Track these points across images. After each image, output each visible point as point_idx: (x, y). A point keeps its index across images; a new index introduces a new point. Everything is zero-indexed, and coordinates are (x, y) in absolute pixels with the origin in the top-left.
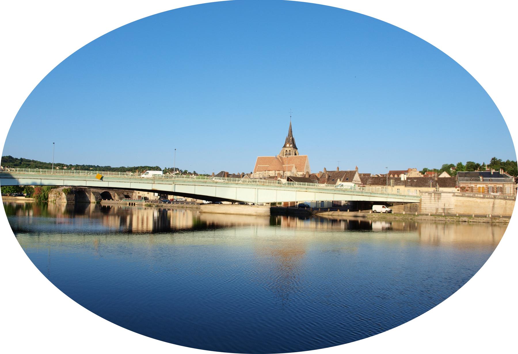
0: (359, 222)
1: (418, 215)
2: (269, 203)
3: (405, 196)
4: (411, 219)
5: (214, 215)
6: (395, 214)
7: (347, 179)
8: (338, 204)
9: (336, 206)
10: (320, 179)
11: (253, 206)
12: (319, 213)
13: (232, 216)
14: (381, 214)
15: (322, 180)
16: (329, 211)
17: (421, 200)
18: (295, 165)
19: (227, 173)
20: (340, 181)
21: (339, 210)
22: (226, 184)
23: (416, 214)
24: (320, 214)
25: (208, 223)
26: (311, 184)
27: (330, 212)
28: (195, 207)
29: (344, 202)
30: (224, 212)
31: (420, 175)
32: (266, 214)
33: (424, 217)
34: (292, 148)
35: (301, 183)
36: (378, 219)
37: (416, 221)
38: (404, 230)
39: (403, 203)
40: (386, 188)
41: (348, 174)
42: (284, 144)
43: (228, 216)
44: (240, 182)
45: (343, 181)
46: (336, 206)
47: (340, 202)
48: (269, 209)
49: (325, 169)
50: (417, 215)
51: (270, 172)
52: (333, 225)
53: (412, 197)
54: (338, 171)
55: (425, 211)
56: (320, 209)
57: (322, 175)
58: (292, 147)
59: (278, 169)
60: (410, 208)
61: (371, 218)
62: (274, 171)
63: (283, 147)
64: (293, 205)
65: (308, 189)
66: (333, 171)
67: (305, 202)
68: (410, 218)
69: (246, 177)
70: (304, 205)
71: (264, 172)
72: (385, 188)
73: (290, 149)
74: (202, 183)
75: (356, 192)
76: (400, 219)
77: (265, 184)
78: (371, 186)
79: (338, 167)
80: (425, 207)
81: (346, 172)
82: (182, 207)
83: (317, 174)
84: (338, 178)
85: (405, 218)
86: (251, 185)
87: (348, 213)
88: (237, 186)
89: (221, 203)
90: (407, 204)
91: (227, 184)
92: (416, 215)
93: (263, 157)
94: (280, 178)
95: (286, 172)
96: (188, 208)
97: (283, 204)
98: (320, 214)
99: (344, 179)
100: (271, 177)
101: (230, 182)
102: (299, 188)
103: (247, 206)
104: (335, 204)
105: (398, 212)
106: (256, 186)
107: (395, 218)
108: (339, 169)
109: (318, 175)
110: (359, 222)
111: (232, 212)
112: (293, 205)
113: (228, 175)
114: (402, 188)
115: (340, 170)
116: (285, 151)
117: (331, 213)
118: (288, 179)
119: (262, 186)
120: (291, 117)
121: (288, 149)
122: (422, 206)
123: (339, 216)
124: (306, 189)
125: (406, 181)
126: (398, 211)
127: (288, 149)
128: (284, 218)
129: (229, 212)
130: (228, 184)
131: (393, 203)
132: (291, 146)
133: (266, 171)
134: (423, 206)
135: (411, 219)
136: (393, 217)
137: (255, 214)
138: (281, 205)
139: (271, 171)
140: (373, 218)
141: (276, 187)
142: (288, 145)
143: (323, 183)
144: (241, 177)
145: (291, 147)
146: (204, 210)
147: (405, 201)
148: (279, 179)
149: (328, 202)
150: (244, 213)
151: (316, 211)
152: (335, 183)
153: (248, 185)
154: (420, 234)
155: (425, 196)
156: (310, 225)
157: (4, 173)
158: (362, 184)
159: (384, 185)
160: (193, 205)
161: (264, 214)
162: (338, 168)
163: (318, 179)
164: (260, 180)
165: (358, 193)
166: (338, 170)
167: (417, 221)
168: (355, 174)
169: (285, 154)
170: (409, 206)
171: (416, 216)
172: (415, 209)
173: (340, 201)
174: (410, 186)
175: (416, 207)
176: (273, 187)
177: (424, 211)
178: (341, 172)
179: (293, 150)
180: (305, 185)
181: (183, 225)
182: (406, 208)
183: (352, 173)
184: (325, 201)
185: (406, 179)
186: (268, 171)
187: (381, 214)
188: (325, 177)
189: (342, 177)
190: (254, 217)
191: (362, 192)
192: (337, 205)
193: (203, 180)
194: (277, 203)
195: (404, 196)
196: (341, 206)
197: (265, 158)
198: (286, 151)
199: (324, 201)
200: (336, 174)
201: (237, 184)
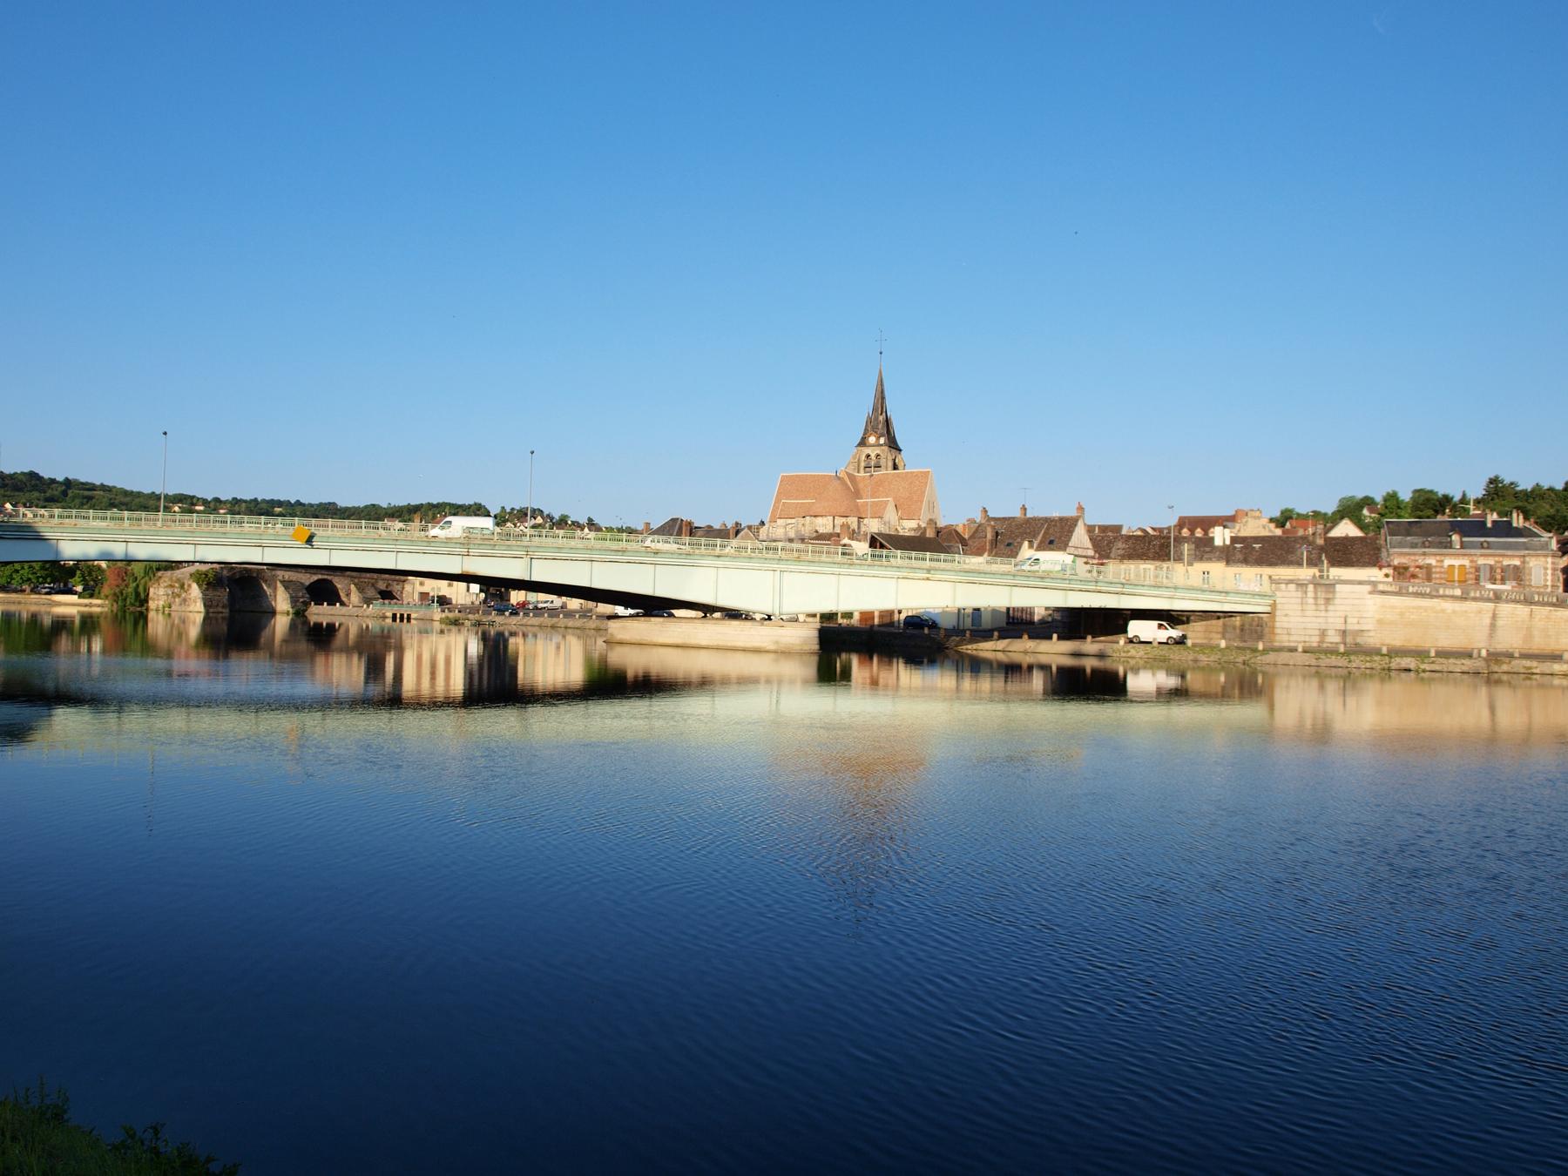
0: (1088, 670)
1: (1265, 651)
2: (814, 616)
3: (1226, 593)
4: (1244, 664)
6: (1197, 649)
7: (1051, 542)
8: (1024, 617)
9: (1018, 623)
10: (970, 542)
11: (768, 622)
12: (966, 645)
13: (703, 652)
14: (1153, 648)
15: (974, 544)
16: (998, 640)
17: (1274, 605)
18: (894, 498)
19: (690, 524)
20: (1031, 546)
21: (1026, 636)
22: (684, 556)
23: (1261, 647)
24: (970, 649)
25: (630, 674)
26: (942, 556)
27: (999, 642)
28: (593, 626)
29: (1043, 612)
30: (679, 641)
31: (1270, 531)
32: (806, 648)
33: (1284, 657)
34: (886, 448)
35: (913, 554)
36: (1146, 662)
37: (1259, 668)
38: (1223, 696)
39: (1218, 614)
40: (1168, 568)
41: (1055, 526)
42: (861, 435)
43: (693, 652)
44: (727, 550)
45: (1039, 548)
46: (1021, 623)
47: (1030, 611)
48: (816, 634)
49: (985, 511)
50: (1264, 650)
51: (819, 520)
52: (1010, 679)
53: (1248, 596)
54: (1023, 517)
55: (1285, 638)
56: (968, 632)
57: (974, 529)
59: (842, 510)
60: (1242, 630)
61: (1122, 659)
64: (888, 621)
65: (932, 572)
66: (1009, 518)
67: (923, 610)
68: (1240, 659)
69: (747, 534)
70: (922, 620)
72: (1165, 569)
73: (878, 452)
75: (1076, 580)
76: (1212, 664)
77: (803, 557)
78: (1125, 561)
79: (1024, 506)
80: (1286, 625)
81: (1046, 520)
82: (553, 627)
83: (961, 525)
84: (1023, 540)
85: (1225, 658)
87: (1055, 644)
88: (719, 563)
89: (672, 615)
90: (1233, 619)
91: (688, 557)
92: (1259, 651)
93: (797, 476)
94: (849, 538)
95: (866, 521)
96: (570, 631)
97: (856, 616)
98: (970, 649)
99: (1041, 542)
100: (820, 537)
101: (697, 551)
102: (908, 570)
103: (748, 624)
104: (1013, 618)
105: (1204, 641)
106: (777, 561)
107: (1196, 661)
108: (1028, 511)
110: (1088, 670)
111: (704, 643)
112: (887, 620)
113: (692, 530)
114: (1217, 569)
115: (1029, 515)
116: (863, 458)
117: (1002, 644)
118: (874, 542)
120: (881, 353)
121: (873, 452)
122: (1277, 624)
123: (1025, 652)
124: (929, 571)
125: (1228, 547)
126: (1205, 638)
127: (873, 452)
128: (860, 659)
129: (693, 641)
131: (1190, 616)
132: (882, 441)
134: (1281, 622)
135: (1244, 664)
136: (1190, 658)
137: (772, 647)
138: (852, 621)
139: (822, 516)
140: (1129, 660)
141: (836, 566)
142: (872, 440)
143: (979, 553)
144: (731, 536)
145: (881, 445)
146: (620, 636)
147: (1227, 608)
148: (846, 541)
149: (995, 611)
150: (740, 644)
151: (958, 639)
152: (1014, 554)
154: (1271, 707)
155: (1285, 594)
156: (939, 681)
157: (322, 574)
158: (1097, 555)
159: (1164, 560)
161: (799, 648)
162: (1024, 509)
163: (964, 542)
164: (788, 545)
165: (1083, 583)
166: (1025, 515)
167: (1263, 669)
168: (1076, 525)
169: (863, 464)
170: (1238, 623)
171: (1258, 654)
172: (1256, 632)
173: (1030, 608)
174: (1241, 562)
175: (1258, 626)
177: (1282, 639)
178: (1034, 519)
180: (924, 559)
182: (1229, 630)
183: (1066, 524)
184: (986, 608)
185: (1228, 542)
187: (1153, 648)
188: (986, 537)
189: (1035, 537)
190: (772, 656)
191: (1097, 582)
192: (1022, 620)
193: (614, 545)
194: (839, 615)
195: (1223, 594)
196: (1031, 623)
197: (802, 479)
198: (868, 456)
199: (982, 609)
200: (1019, 526)
201: (718, 556)
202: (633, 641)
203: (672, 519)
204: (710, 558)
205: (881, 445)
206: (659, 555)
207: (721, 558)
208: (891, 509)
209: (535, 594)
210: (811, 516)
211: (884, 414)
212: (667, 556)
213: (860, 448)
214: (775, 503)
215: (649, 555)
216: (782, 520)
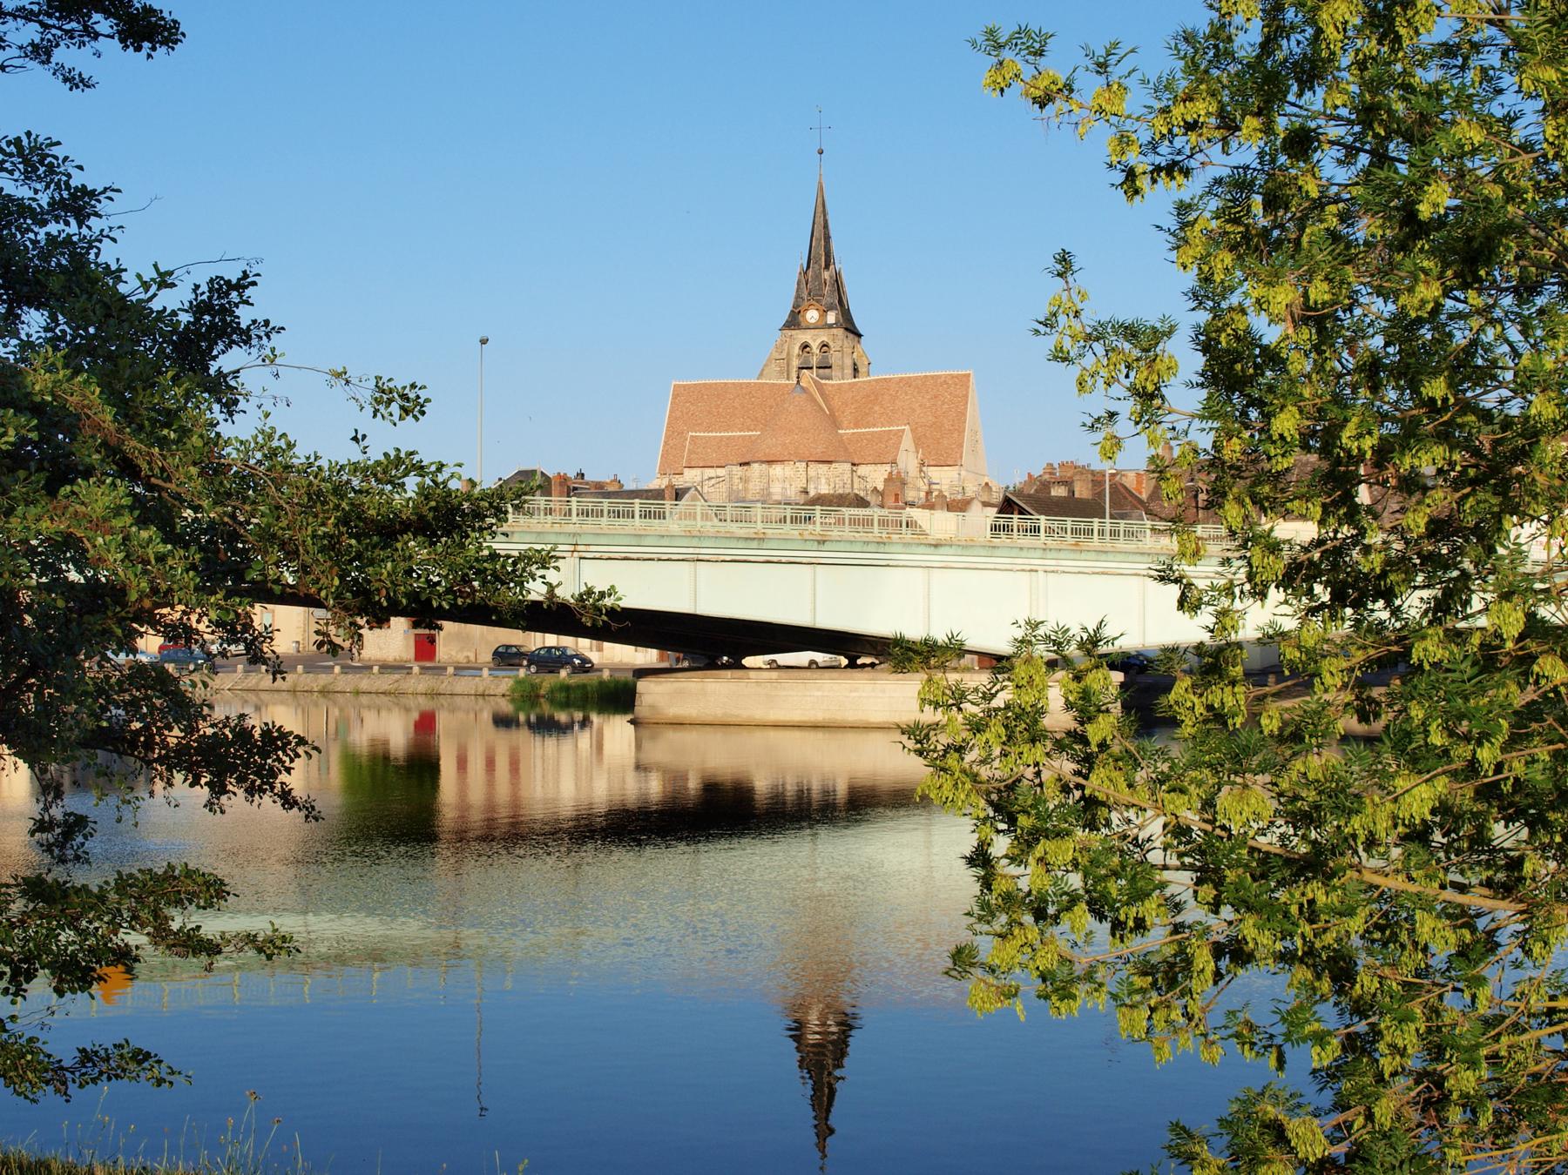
22: (872, 548)
25: (762, 785)
28: (421, 688)
30: (819, 716)
34: (840, 332)
43: (851, 738)
58: (837, 325)
59: (819, 451)
62: (804, 464)
63: (781, 326)
71: (738, 471)
73: (825, 339)
77: (1084, 546)
82: (324, 692)
83: (1132, 475)
86: (1015, 553)
88: (935, 558)
96: (364, 699)
101: (895, 537)
106: (1039, 553)
109: (1139, 483)
116: (796, 350)
119: (1072, 556)
120: (821, 152)
121: (815, 339)
127: (815, 339)
129: (851, 716)
130: (887, 549)
132: (831, 318)
133: (755, 466)
142: (812, 316)
145: (830, 326)
153: (997, 552)
169: (795, 363)
176: (1131, 558)
186: (764, 466)
197: (719, 391)
201: (936, 546)
202: (709, 719)
203: (520, 473)
204: (922, 549)
205: (830, 326)
206: (827, 546)
207: (941, 550)
208: (907, 442)
210: (763, 462)
211: (832, 267)
212: (841, 547)
213: (789, 333)
214: (667, 437)
215: (809, 545)
216: (697, 472)
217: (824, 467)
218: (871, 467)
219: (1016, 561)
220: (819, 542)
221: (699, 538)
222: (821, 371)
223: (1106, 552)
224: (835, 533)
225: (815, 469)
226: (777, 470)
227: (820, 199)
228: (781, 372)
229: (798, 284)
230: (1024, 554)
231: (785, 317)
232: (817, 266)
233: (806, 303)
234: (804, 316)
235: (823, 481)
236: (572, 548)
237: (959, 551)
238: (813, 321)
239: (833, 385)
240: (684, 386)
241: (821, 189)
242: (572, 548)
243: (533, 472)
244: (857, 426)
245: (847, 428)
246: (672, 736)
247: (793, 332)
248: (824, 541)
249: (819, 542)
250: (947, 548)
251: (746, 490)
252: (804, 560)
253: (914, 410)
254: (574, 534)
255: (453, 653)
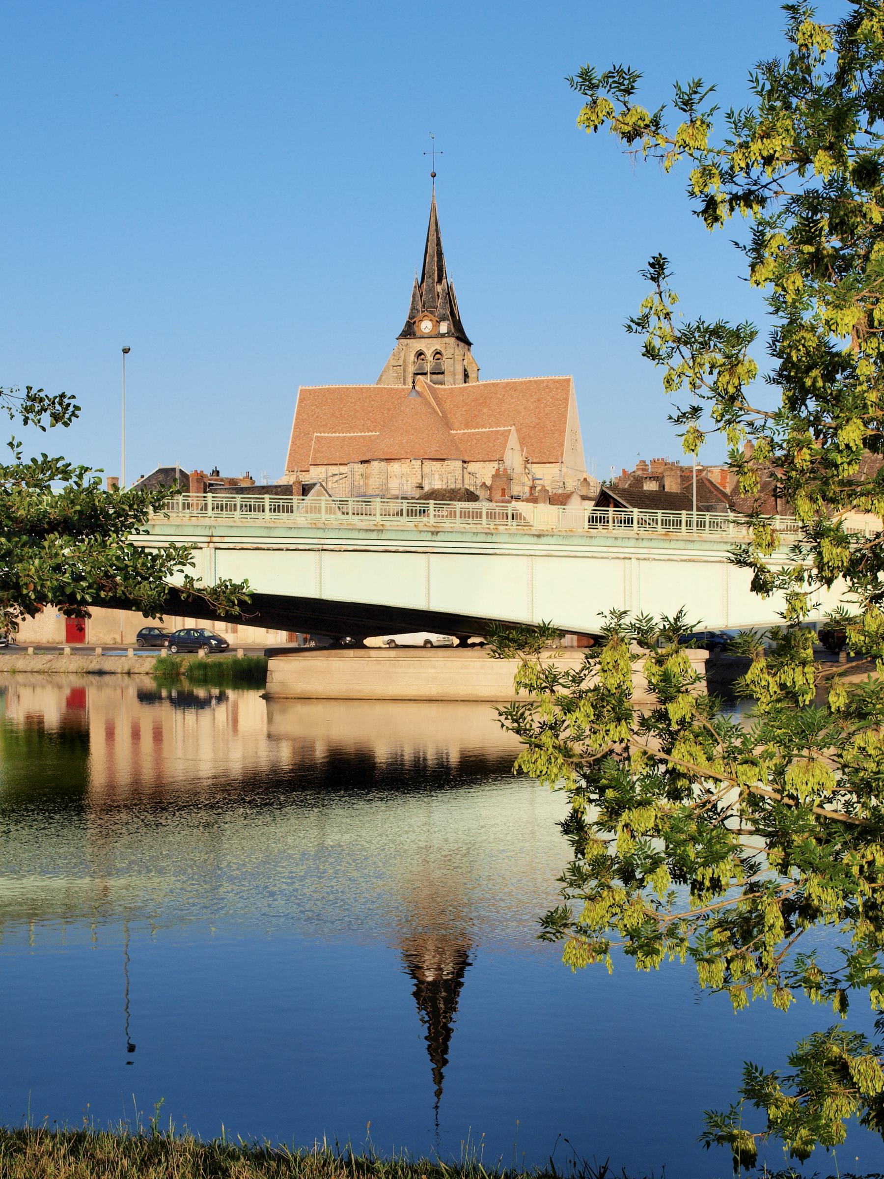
5: (365, 710)
22: (481, 538)
25: (382, 753)
28: (73, 667)
30: (432, 690)
34: (452, 341)
42: (406, 319)
43: (462, 710)
58: (449, 334)
59: (433, 450)
62: (419, 462)
63: (397, 336)
71: (359, 468)
73: (439, 347)
74: (362, 535)
77: (673, 536)
83: (717, 471)
86: (610, 542)
88: (541, 546)
93: (328, 390)
96: (20, 678)
101: (502, 528)
106: (633, 543)
109: (724, 478)
116: (412, 357)
119: (663, 545)
121: (429, 347)
127: (429, 347)
130: (494, 539)
132: (444, 328)
133: (375, 464)
142: (426, 326)
146: (301, 687)
160: (50, 657)
169: (411, 369)
176: (715, 547)
179: (457, 350)
181: (159, 777)
198: (420, 354)
201: (539, 536)
202: (333, 694)
203: (161, 471)
204: (526, 539)
206: (440, 537)
207: (544, 540)
208: (513, 441)
209: (179, 618)
210: (382, 460)
211: (444, 281)
213: (405, 341)
214: (295, 438)
216: (322, 469)
217: (438, 464)
218: (479, 465)
219: (612, 550)
220: (433, 533)
221: (324, 529)
222: (435, 377)
223: (694, 541)
224: (447, 524)
225: (429, 466)
226: (395, 467)
227: (433, 219)
228: (398, 378)
229: (414, 296)
230: (619, 543)
231: (401, 327)
232: (430, 281)
233: (421, 315)
234: (419, 327)
235: (437, 477)
236: (207, 539)
237: (560, 541)
238: (427, 331)
239: (445, 390)
240: (310, 391)
241: (434, 209)
242: (207, 539)
243: (174, 470)
244: (467, 426)
245: (458, 429)
246: (301, 710)
247: (409, 341)
248: (437, 532)
249: (433, 533)
250: (549, 538)
251: (366, 485)
252: (419, 549)
253: (519, 412)
254: (210, 527)
255: (101, 635)
